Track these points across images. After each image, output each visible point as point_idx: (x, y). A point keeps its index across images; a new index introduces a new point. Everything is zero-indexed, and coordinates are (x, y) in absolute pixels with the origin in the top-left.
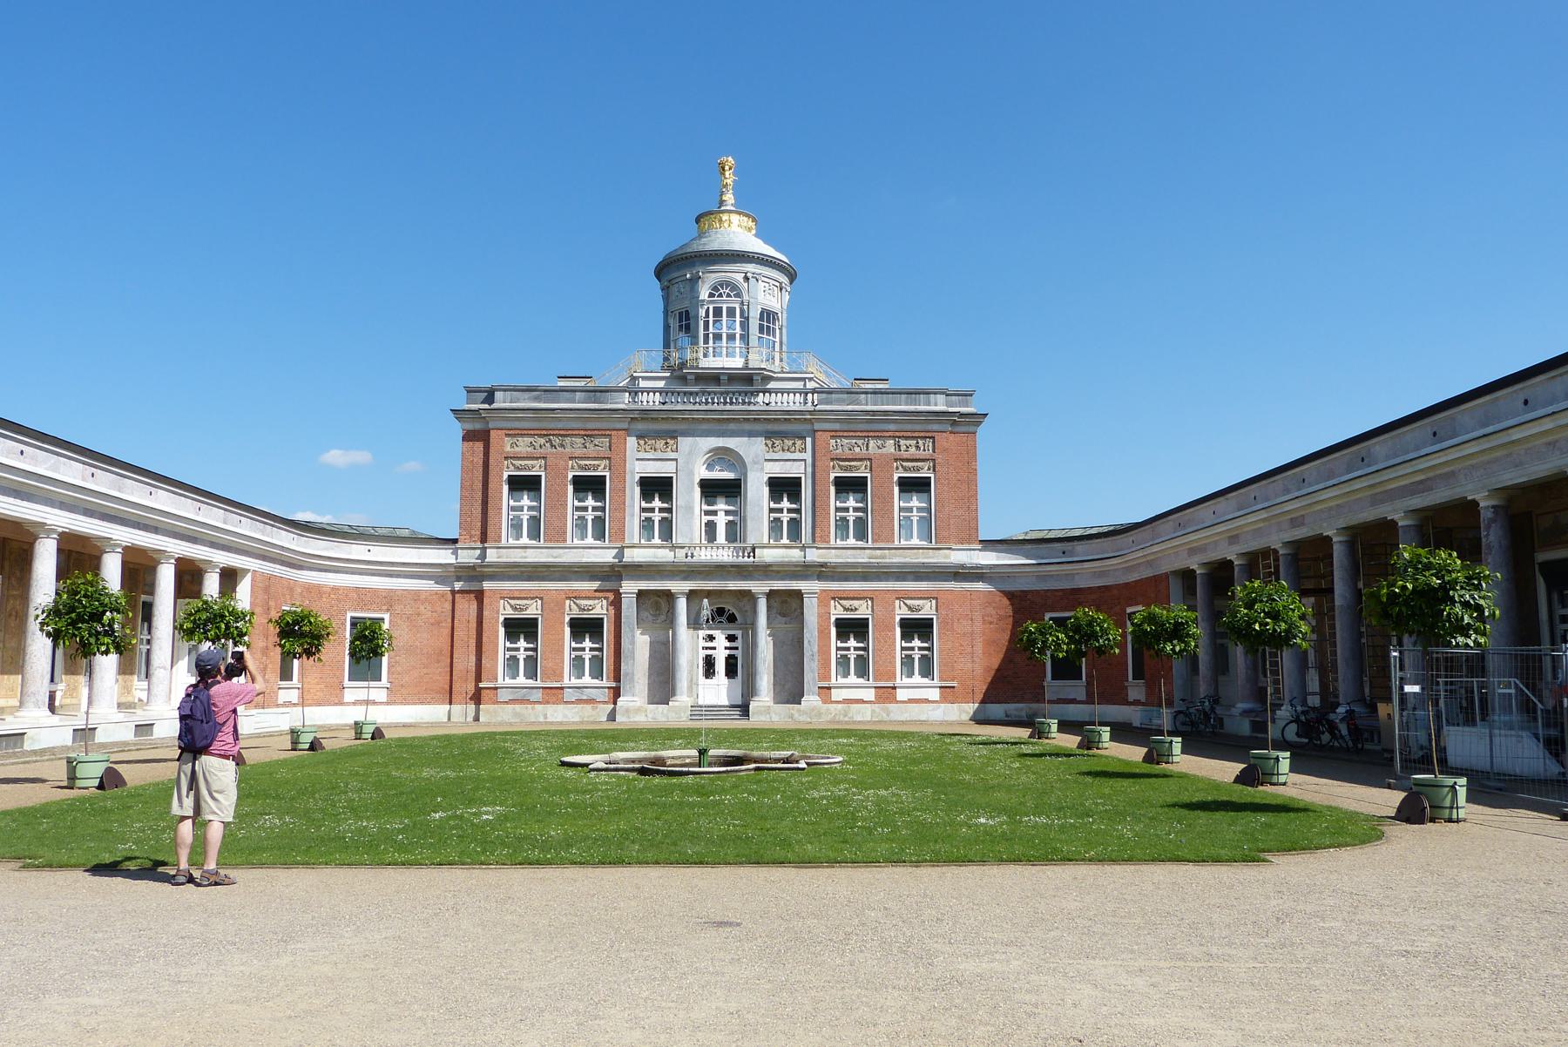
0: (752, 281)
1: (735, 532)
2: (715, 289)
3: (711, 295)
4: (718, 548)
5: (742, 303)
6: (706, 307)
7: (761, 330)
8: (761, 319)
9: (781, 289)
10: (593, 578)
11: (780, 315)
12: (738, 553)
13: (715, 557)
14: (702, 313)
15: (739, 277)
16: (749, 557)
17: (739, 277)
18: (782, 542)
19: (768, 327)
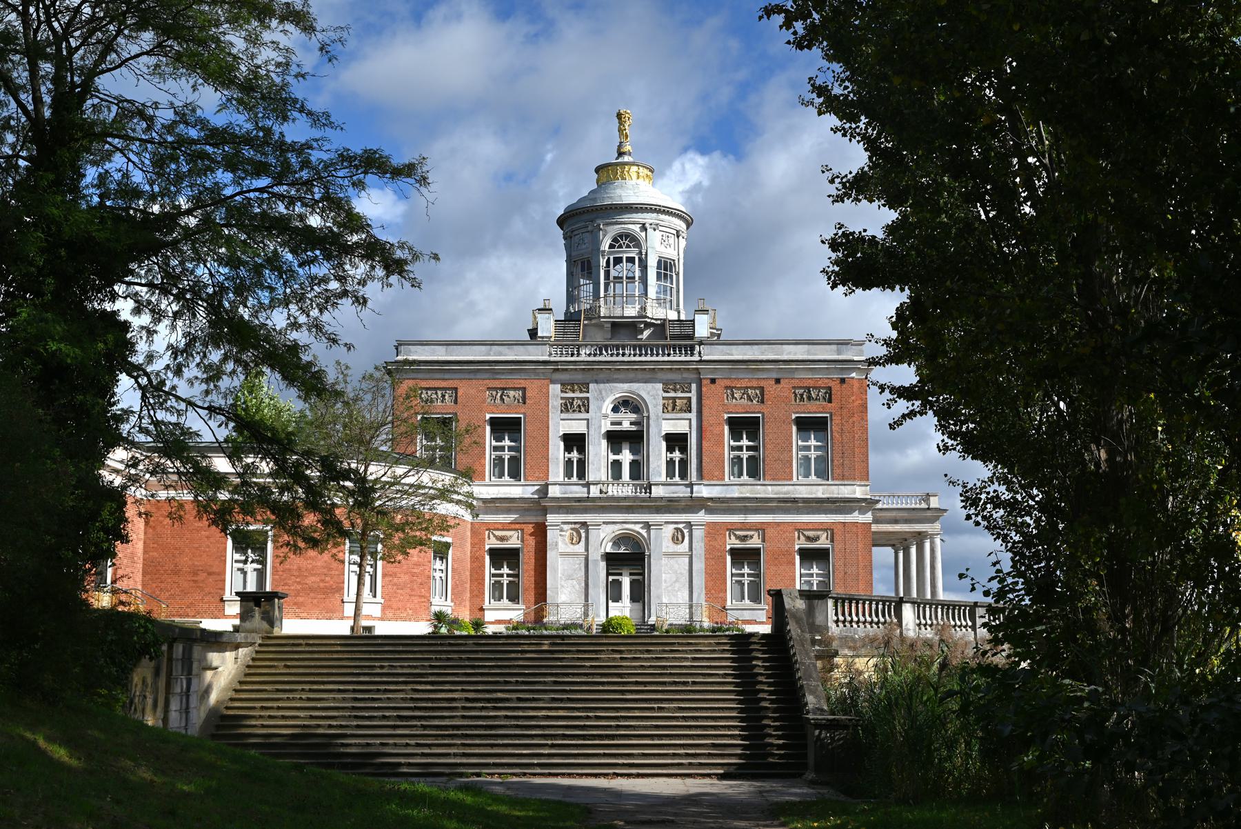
0: (650, 231)
1: (637, 470)
2: (615, 240)
3: (611, 246)
4: (623, 485)
5: (640, 253)
6: (606, 258)
7: (659, 274)
8: (659, 267)
9: (678, 237)
10: (508, 511)
11: (676, 262)
12: (636, 489)
13: (615, 493)
14: (603, 262)
15: (637, 228)
16: (645, 493)
17: (637, 228)
18: (674, 480)
19: (666, 275)
